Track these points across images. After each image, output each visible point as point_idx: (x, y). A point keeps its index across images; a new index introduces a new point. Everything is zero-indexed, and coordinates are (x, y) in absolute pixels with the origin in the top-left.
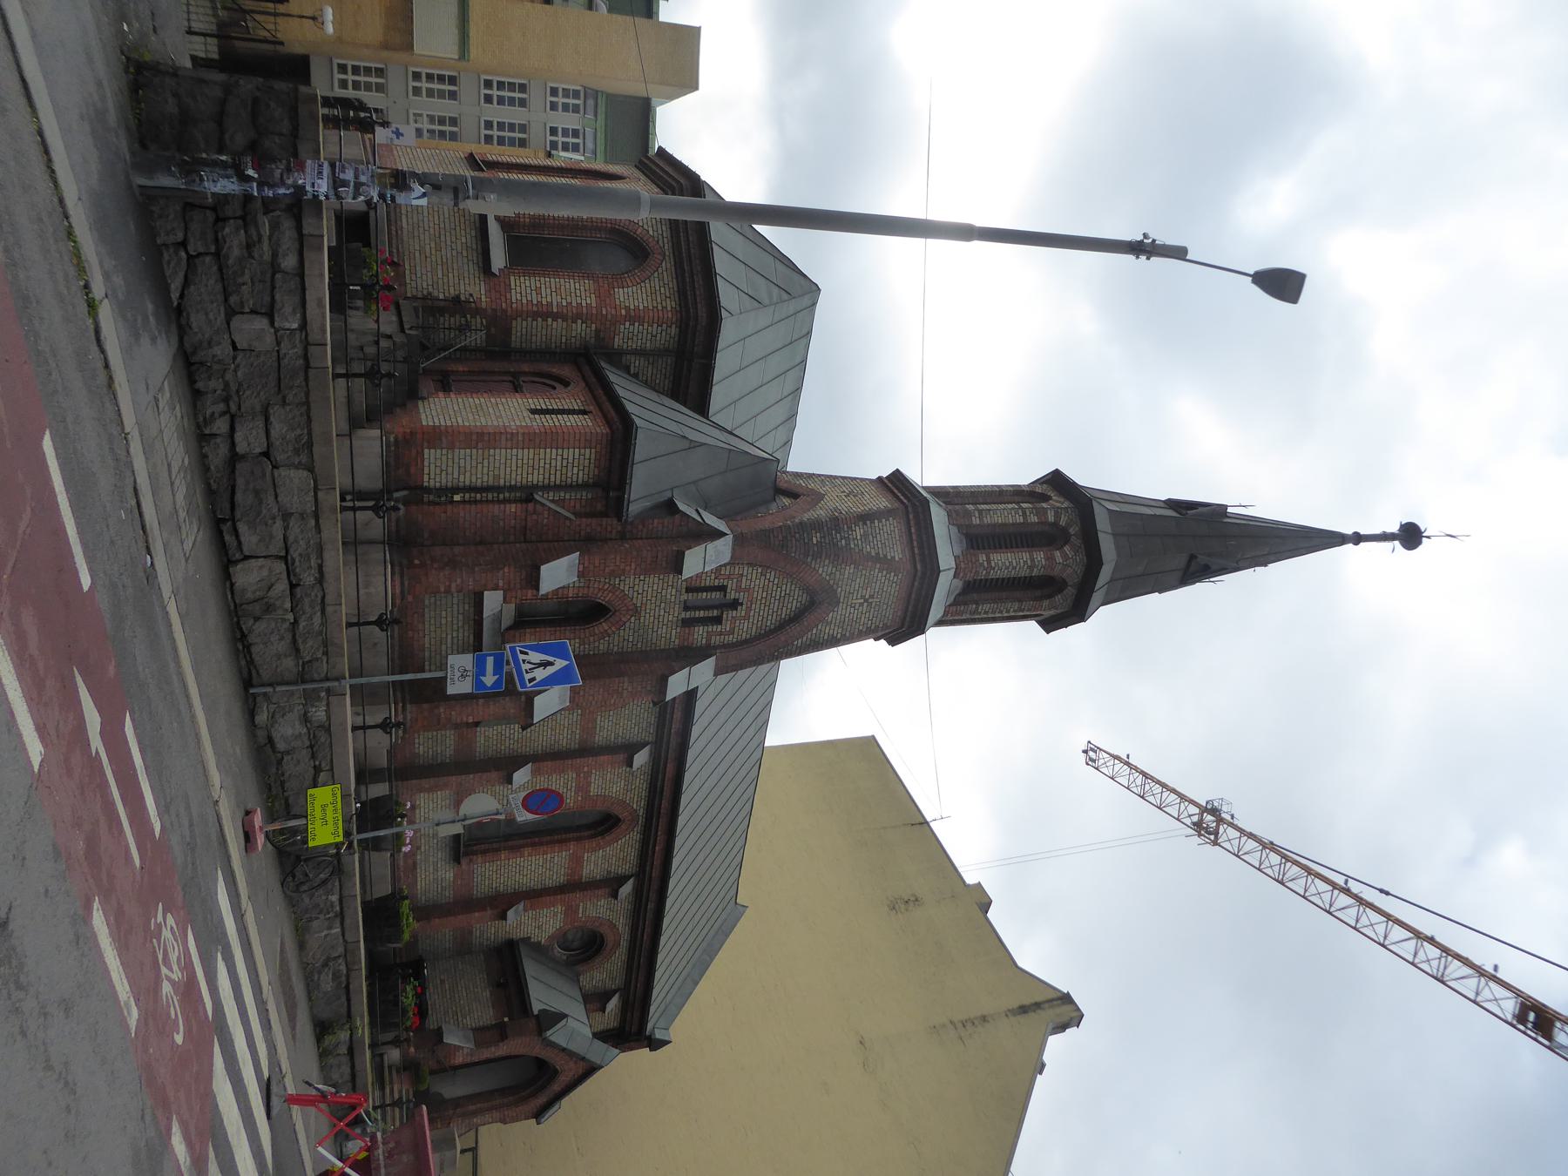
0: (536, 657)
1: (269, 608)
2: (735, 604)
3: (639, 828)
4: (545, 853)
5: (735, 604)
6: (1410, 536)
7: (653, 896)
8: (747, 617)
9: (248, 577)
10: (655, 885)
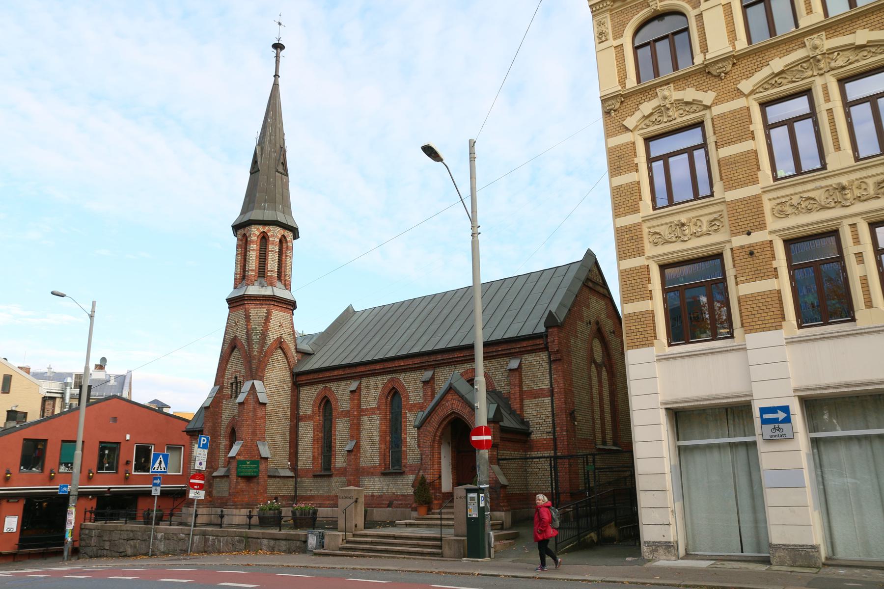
0: (157, 465)
1: (135, 547)
2: (236, 378)
3: (398, 376)
4: (406, 426)
5: (236, 378)
6: (278, 47)
7: (432, 358)
8: (239, 372)
9: (129, 551)
10: (426, 359)
